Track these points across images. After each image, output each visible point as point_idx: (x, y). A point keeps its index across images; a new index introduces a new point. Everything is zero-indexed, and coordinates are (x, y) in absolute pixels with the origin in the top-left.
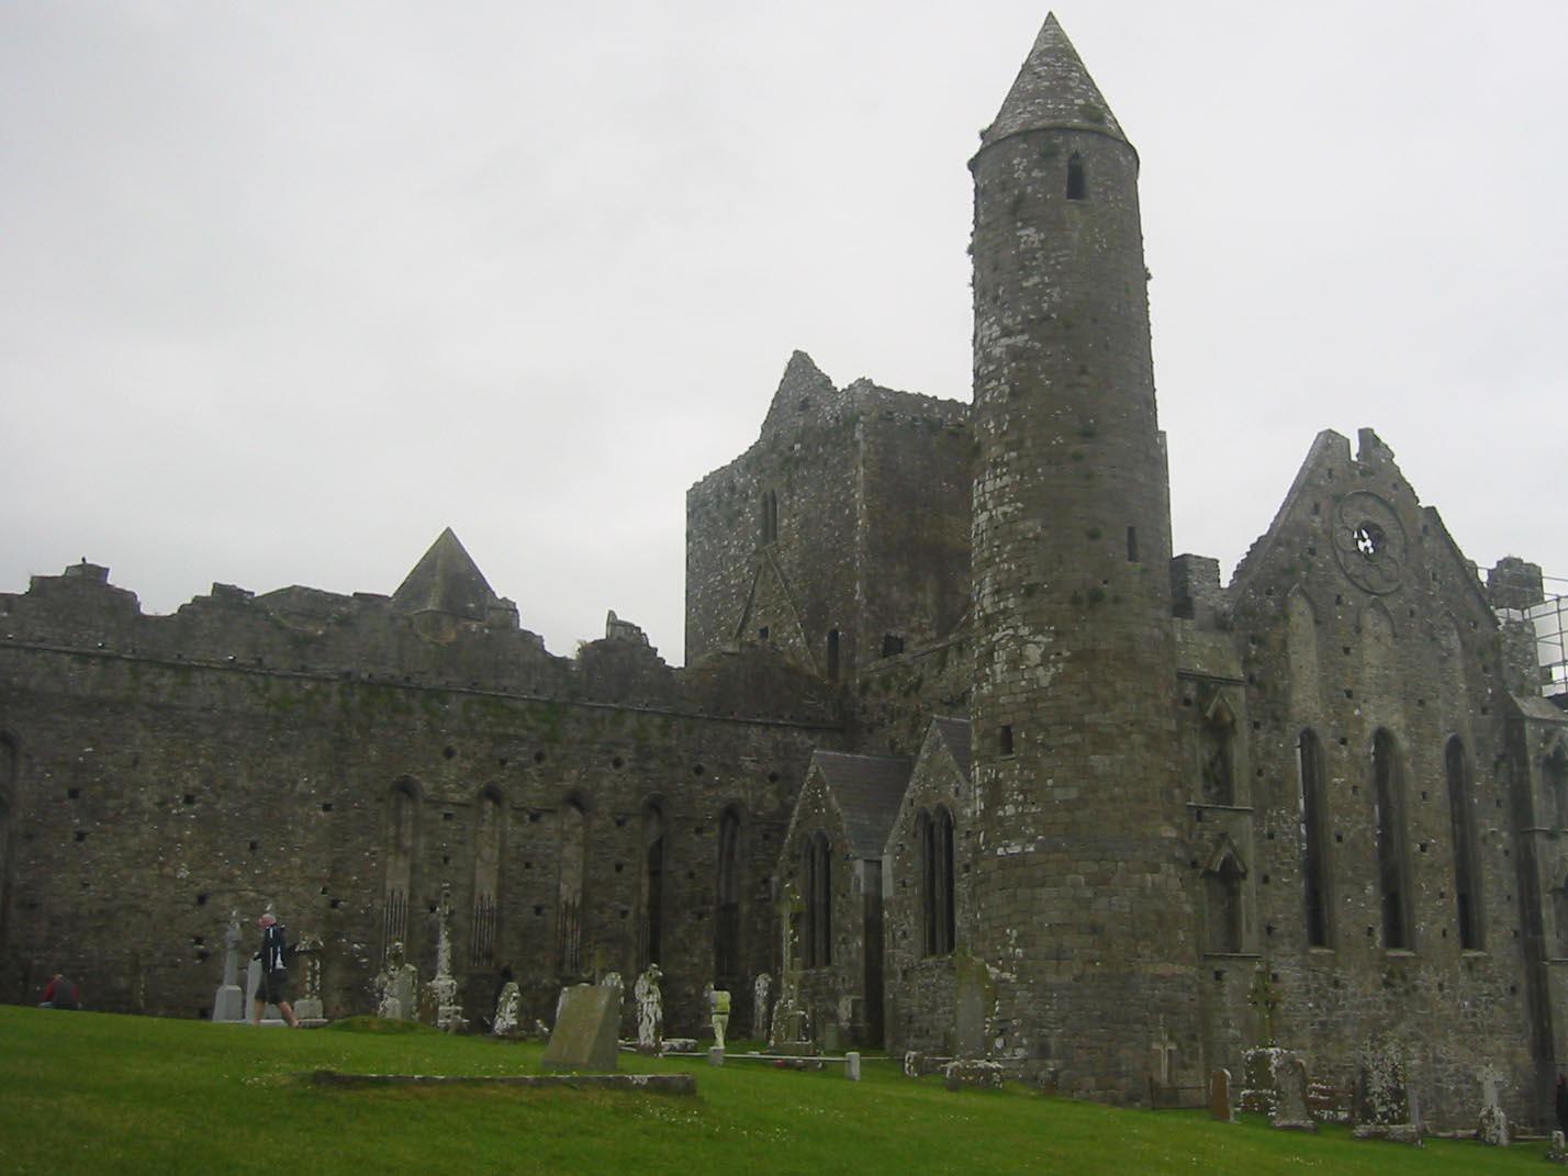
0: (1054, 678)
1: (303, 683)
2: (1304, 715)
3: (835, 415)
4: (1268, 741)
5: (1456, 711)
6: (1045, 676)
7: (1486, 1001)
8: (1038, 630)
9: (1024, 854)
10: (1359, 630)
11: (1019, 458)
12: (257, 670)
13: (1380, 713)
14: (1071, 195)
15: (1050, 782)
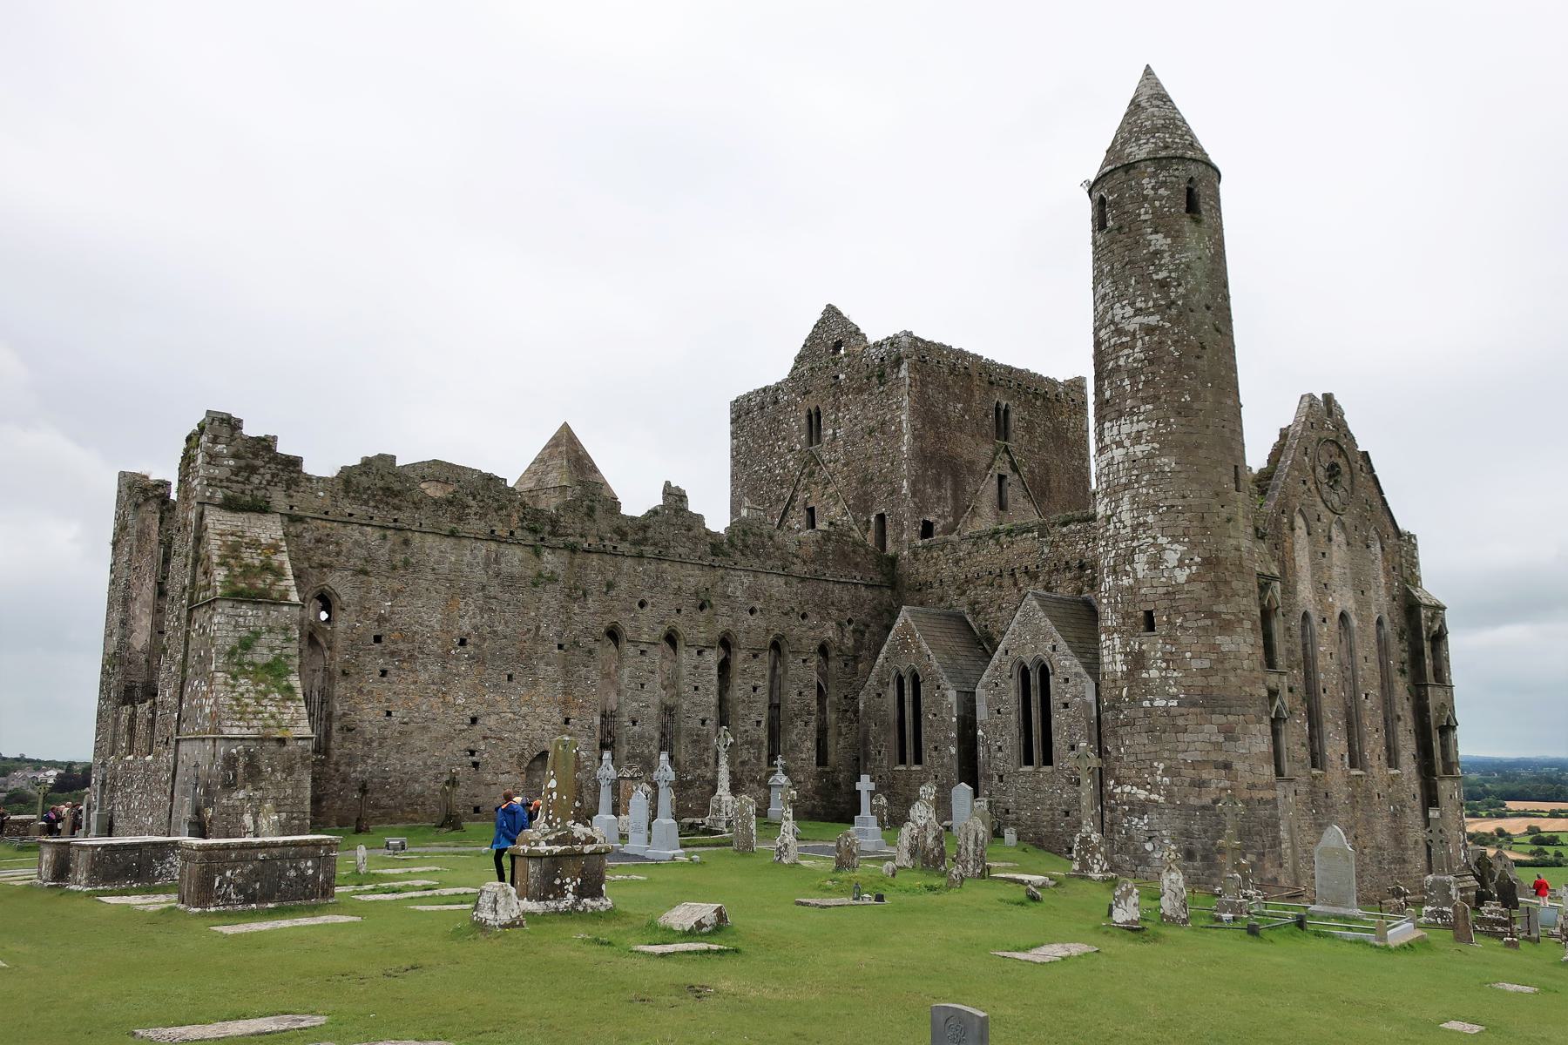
0: (1188, 576)
3: (880, 356)
5: (1381, 601)
6: (1181, 576)
8: (1175, 539)
9: (1167, 709)
10: (1330, 539)
13: (1343, 600)
14: (1188, 211)
15: (1188, 655)
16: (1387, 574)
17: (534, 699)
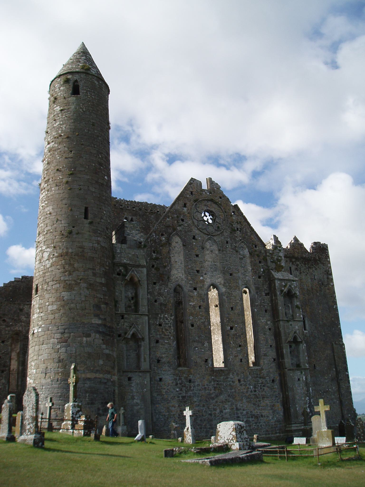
0: (52, 264)
2: (177, 279)
4: (160, 289)
7: (261, 386)
11: (48, 185)
16: (253, 265)
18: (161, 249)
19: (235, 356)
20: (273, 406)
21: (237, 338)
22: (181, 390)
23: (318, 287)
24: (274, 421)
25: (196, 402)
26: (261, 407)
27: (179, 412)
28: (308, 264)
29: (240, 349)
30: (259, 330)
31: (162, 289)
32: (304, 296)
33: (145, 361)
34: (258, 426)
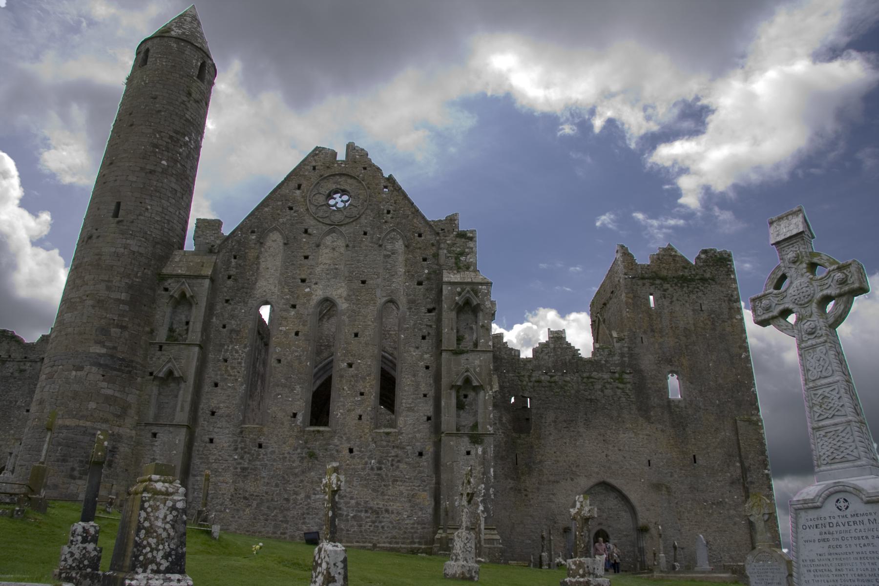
1: (27, 363)
2: (265, 294)
7: (393, 460)
12: (9, 359)
17: (7, 437)
18: (246, 253)
19: (349, 411)
20: (413, 496)
21: (356, 381)
22: (242, 458)
23: (707, 324)
24: (412, 522)
25: (264, 478)
26: (389, 496)
27: (232, 490)
28: (688, 287)
29: (359, 399)
30: (404, 369)
31: (236, 308)
32: (677, 340)
33: (182, 409)
34: (378, 527)
